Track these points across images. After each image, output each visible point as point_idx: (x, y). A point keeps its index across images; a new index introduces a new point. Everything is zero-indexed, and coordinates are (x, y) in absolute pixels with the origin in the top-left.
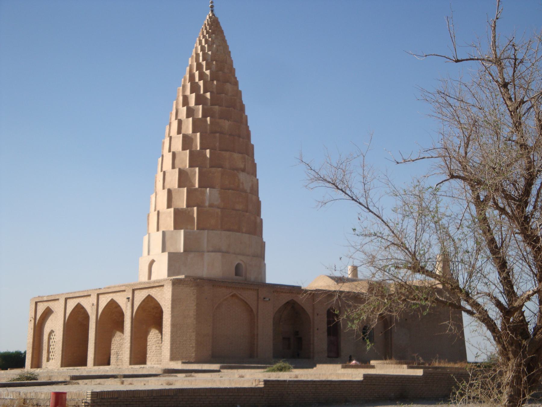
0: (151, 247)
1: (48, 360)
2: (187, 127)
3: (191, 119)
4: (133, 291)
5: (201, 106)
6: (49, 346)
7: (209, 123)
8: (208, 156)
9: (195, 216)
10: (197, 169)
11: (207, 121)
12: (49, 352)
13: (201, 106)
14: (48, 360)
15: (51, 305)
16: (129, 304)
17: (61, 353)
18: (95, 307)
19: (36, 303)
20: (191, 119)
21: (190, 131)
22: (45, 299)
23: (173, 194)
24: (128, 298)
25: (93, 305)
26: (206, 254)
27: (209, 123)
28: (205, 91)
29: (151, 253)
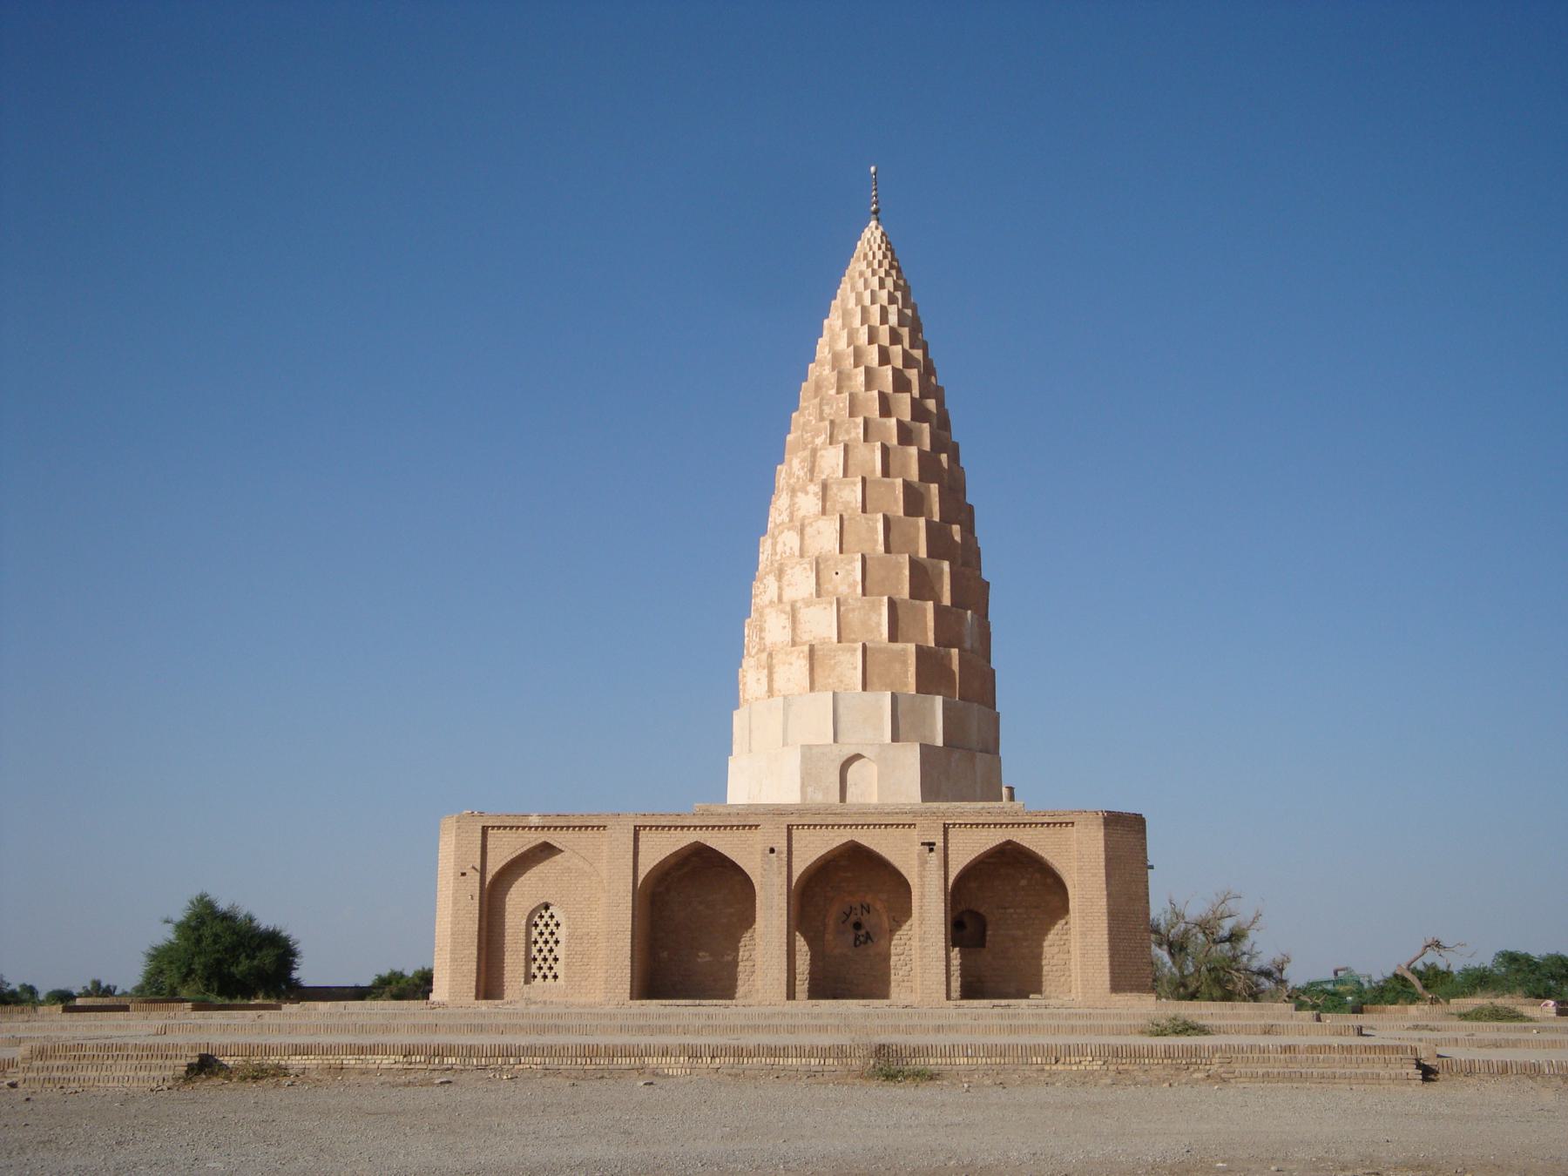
0: (842, 726)
1: (529, 978)
2: (905, 466)
3: (913, 450)
4: (946, 828)
5: (926, 426)
6: (530, 943)
7: (945, 465)
8: (958, 538)
9: (955, 666)
10: (946, 565)
11: (940, 461)
12: (530, 960)
13: (926, 426)
14: (529, 978)
15: (554, 838)
16: (935, 859)
17: (628, 962)
18: (785, 855)
19: (485, 830)
20: (913, 450)
21: (914, 474)
22: (535, 820)
23: (900, 612)
24: (931, 846)
25: (772, 851)
26: (979, 755)
27: (945, 465)
28: (923, 395)
29: (841, 738)
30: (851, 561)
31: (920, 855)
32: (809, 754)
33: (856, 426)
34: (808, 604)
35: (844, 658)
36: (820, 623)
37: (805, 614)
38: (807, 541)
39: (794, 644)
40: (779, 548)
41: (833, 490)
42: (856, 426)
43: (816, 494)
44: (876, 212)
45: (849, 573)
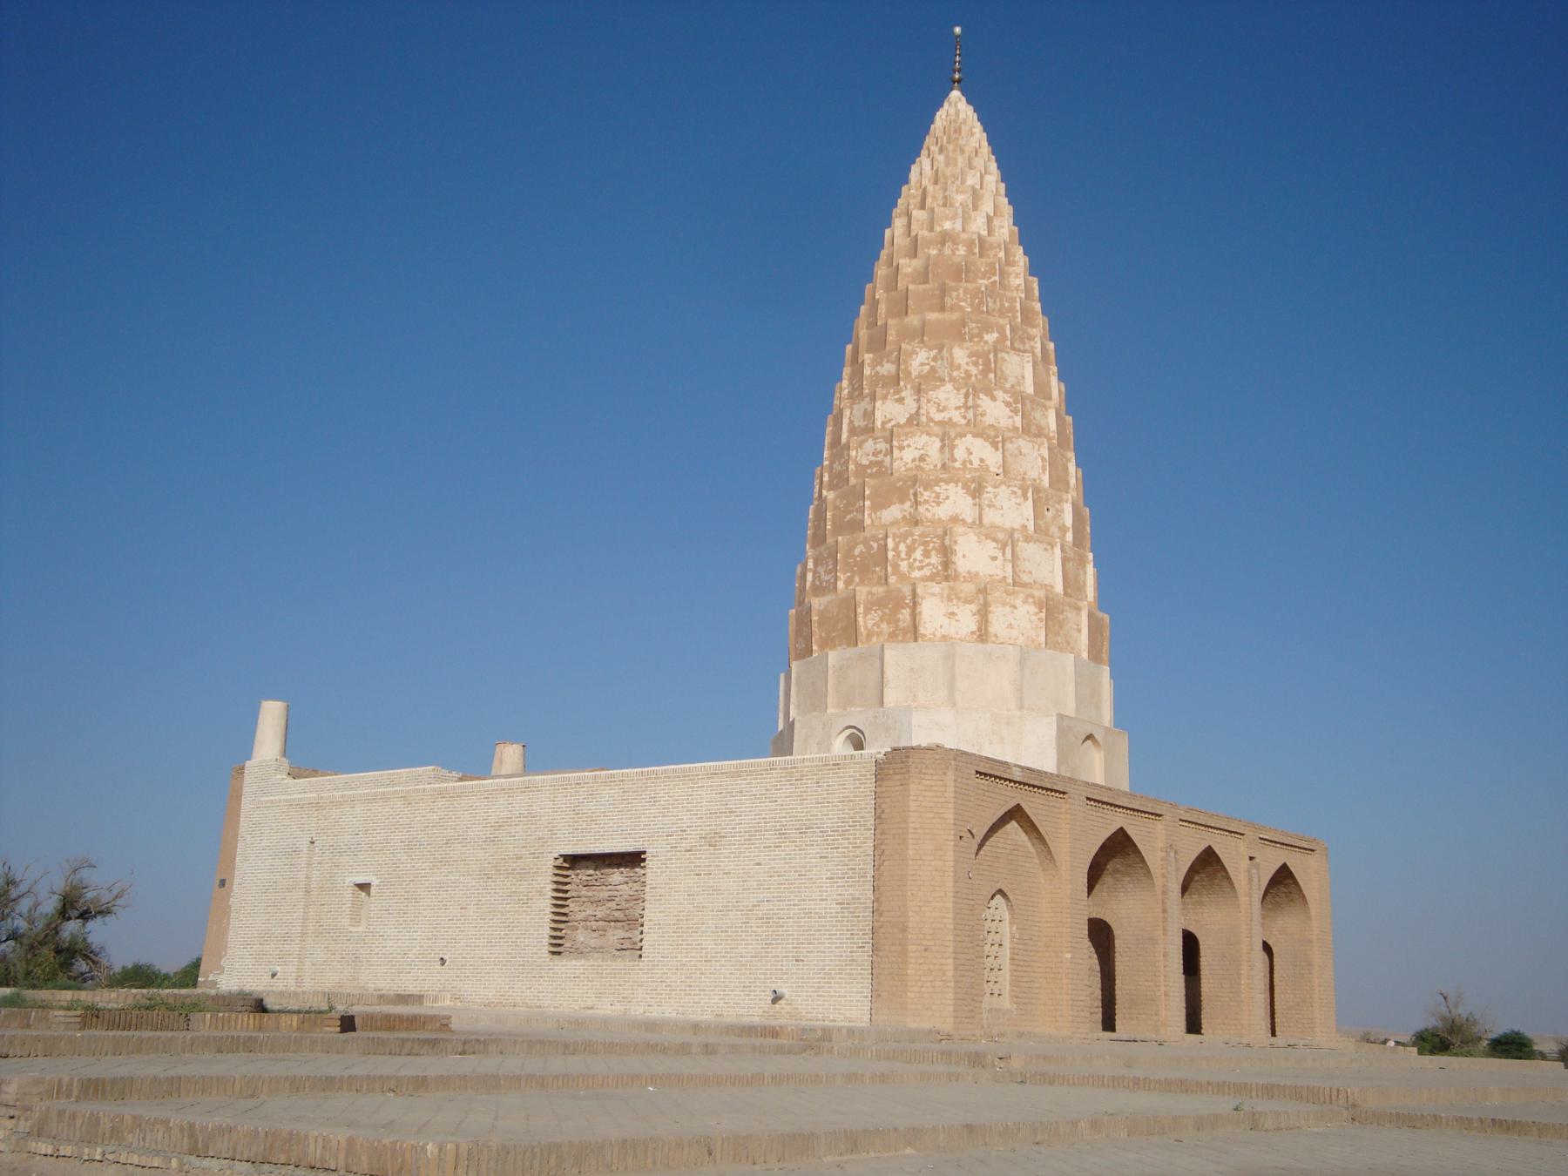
30: (1060, 501)
31: (1249, 870)
32: (1063, 732)
33: (1031, 338)
34: (1028, 539)
35: (1070, 614)
36: (1046, 566)
37: (1028, 550)
38: (1010, 460)
39: (1015, 584)
40: (960, 453)
41: (1028, 407)
42: (1031, 338)
43: (1008, 404)
44: (959, 81)
45: (1059, 512)
